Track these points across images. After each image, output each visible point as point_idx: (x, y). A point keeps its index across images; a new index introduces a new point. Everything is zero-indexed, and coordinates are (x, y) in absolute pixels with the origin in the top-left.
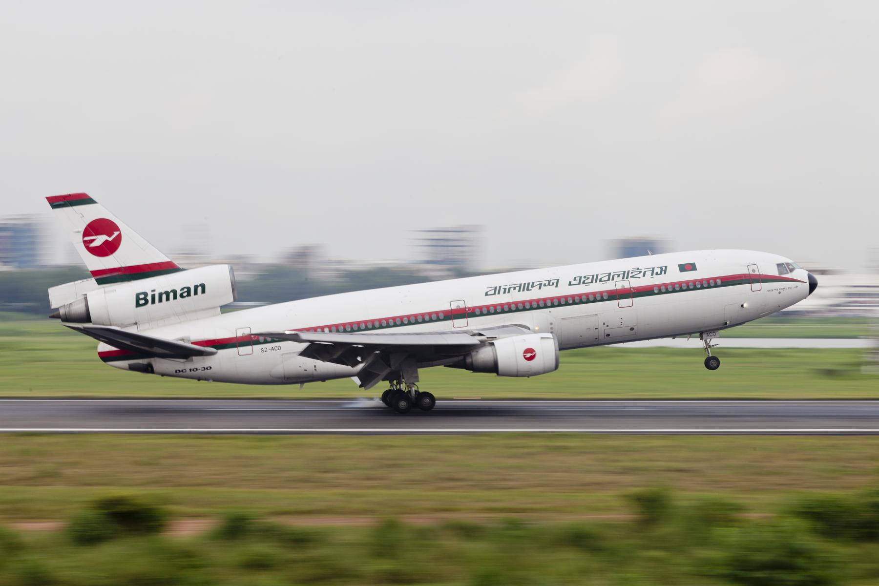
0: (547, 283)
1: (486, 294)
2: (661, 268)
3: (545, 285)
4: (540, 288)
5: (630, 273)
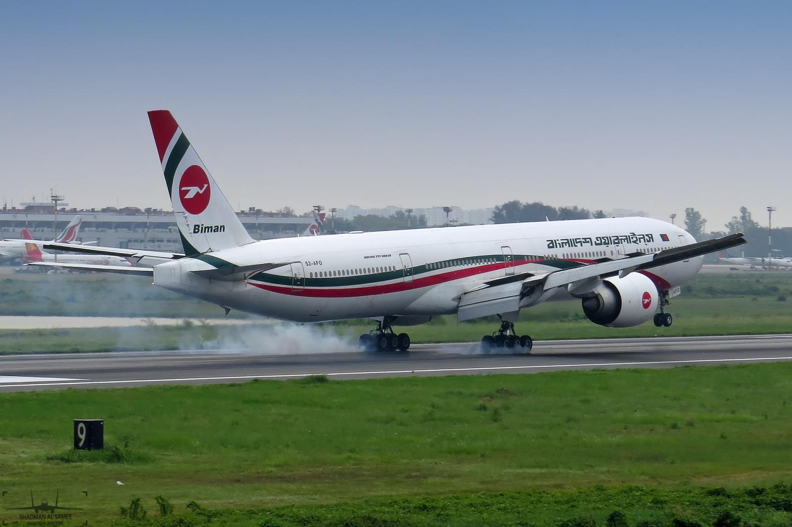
3: (584, 242)
4: (582, 245)
5: (631, 237)
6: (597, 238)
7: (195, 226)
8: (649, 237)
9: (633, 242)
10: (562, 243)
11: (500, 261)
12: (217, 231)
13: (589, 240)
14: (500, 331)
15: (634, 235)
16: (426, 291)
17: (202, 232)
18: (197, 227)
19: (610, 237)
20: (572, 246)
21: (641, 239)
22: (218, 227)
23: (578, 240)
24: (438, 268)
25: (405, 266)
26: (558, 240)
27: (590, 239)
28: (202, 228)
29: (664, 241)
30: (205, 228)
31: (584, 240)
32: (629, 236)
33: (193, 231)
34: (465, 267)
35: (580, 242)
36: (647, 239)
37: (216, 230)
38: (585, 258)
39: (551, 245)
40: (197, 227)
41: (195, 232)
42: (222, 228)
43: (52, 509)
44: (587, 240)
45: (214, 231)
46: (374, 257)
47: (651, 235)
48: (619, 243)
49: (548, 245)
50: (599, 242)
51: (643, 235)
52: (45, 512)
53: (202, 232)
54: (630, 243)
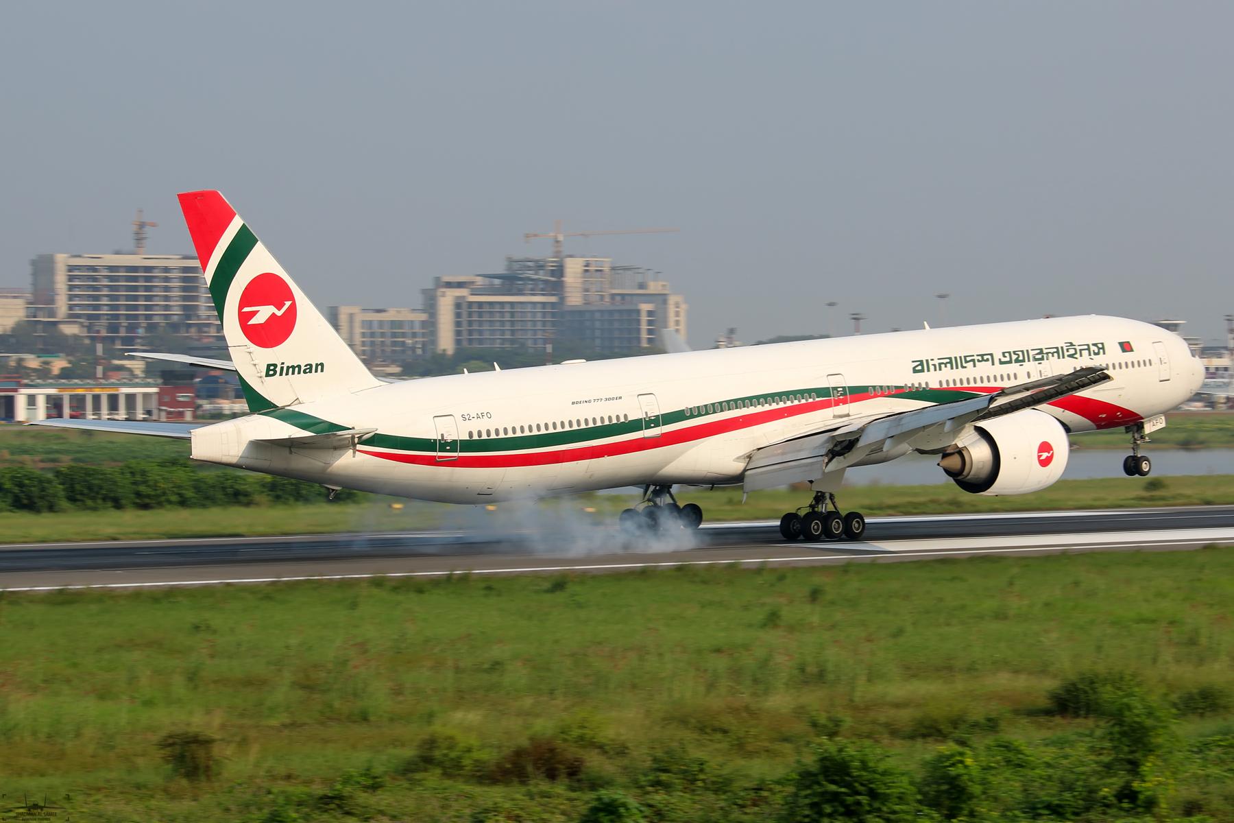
3: (979, 361)
4: (975, 366)
5: (1065, 349)
6: (1004, 353)
7: (269, 366)
8: (1098, 347)
9: (1069, 356)
10: (940, 364)
11: (823, 397)
12: (310, 372)
13: (989, 357)
14: (811, 506)
15: (1071, 344)
16: (682, 453)
17: (281, 374)
18: (272, 368)
19: (1027, 351)
20: (957, 368)
21: (1083, 352)
22: (311, 365)
23: (968, 359)
24: (707, 414)
25: (646, 413)
26: (932, 360)
27: (991, 355)
28: (282, 368)
29: (1123, 352)
30: (288, 368)
31: (980, 358)
32: (1062, 348)
33: (264, 374)
34: (759, 409)
35: (973, 360)
36: (1094, 351)
37: (308, 371)
38: (979, 384)
39: (920, 368)
40: (272, 368)
41: (268, 375)
42: (320, 367)
43: (42, 808)
44: (985, 357)
45: (305, 372)
46: (590, 401)
47: (1102, 344)
48: (1042, 359)
49: (914, 368)
50: (1007, 359)
51: (1088, 345)
52: (35, 811)
53: (281, 374)
54: (1063, 357)
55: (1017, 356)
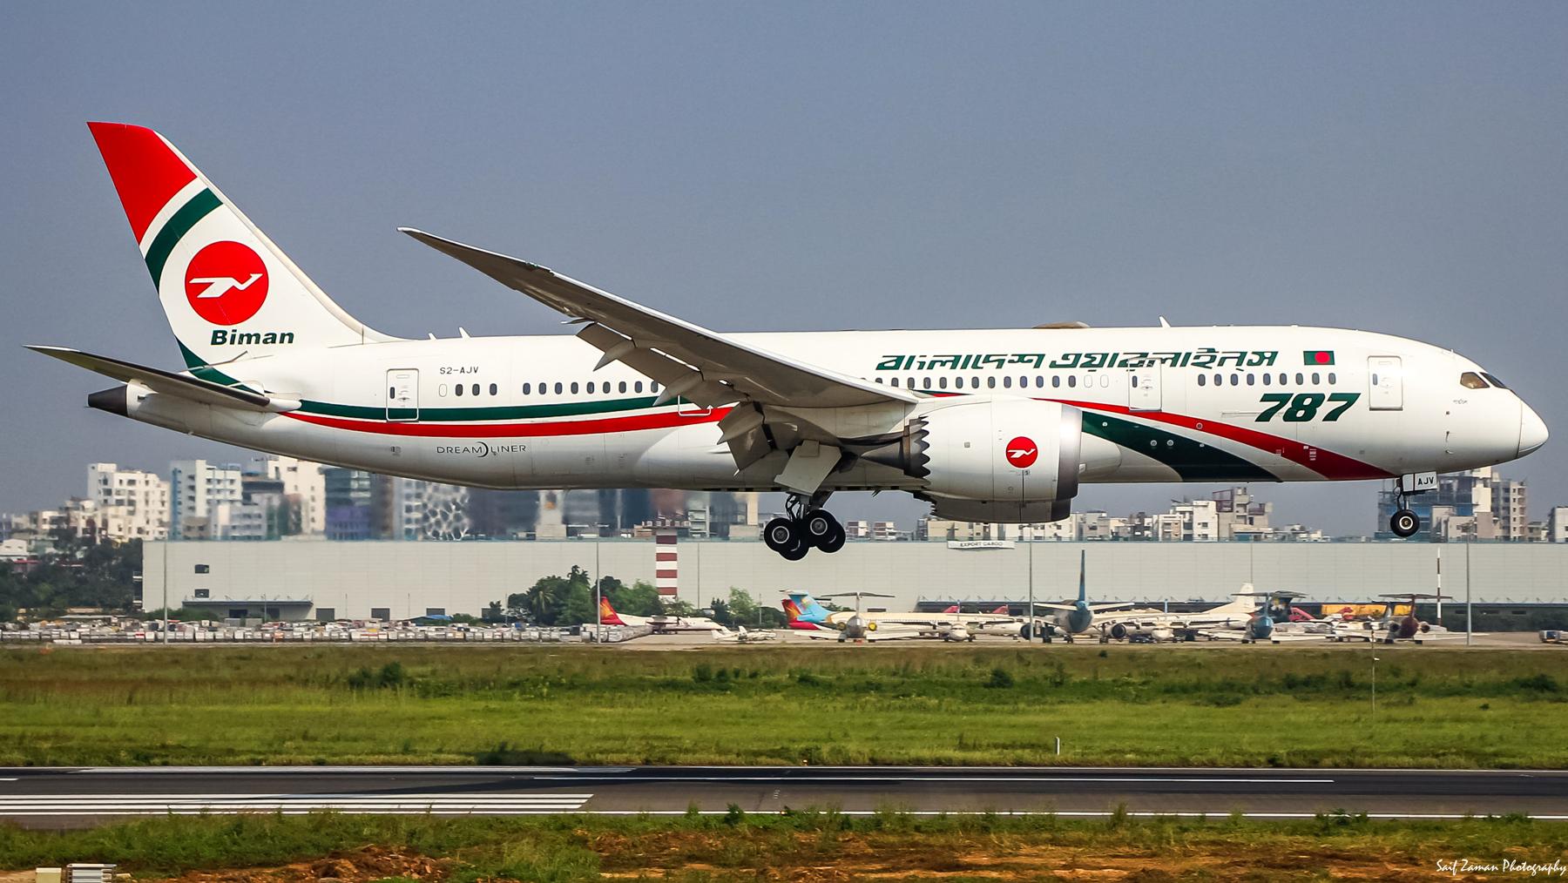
0: (1016, 358)
1: (881, 367)
2: (1261, 354)
3: (1011, 361)
4: (999, 367)
9: (1193, 364)
17: (232, 342)
18: (220, 335)
23: (991, 359)
28: (233, 337)
30: (242, 336)
37: (269, 341)
39: (893, 364)
40: (220, 335)
41: (214, 342)
45: (265, 342)
48: (1141, 364)
50: (1069, 362)
53: (232, 342)
55: (1089, 359)
